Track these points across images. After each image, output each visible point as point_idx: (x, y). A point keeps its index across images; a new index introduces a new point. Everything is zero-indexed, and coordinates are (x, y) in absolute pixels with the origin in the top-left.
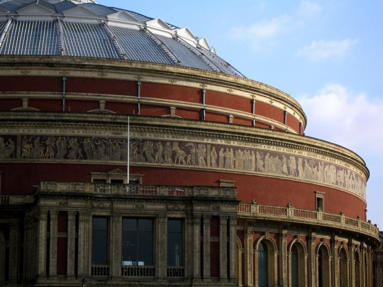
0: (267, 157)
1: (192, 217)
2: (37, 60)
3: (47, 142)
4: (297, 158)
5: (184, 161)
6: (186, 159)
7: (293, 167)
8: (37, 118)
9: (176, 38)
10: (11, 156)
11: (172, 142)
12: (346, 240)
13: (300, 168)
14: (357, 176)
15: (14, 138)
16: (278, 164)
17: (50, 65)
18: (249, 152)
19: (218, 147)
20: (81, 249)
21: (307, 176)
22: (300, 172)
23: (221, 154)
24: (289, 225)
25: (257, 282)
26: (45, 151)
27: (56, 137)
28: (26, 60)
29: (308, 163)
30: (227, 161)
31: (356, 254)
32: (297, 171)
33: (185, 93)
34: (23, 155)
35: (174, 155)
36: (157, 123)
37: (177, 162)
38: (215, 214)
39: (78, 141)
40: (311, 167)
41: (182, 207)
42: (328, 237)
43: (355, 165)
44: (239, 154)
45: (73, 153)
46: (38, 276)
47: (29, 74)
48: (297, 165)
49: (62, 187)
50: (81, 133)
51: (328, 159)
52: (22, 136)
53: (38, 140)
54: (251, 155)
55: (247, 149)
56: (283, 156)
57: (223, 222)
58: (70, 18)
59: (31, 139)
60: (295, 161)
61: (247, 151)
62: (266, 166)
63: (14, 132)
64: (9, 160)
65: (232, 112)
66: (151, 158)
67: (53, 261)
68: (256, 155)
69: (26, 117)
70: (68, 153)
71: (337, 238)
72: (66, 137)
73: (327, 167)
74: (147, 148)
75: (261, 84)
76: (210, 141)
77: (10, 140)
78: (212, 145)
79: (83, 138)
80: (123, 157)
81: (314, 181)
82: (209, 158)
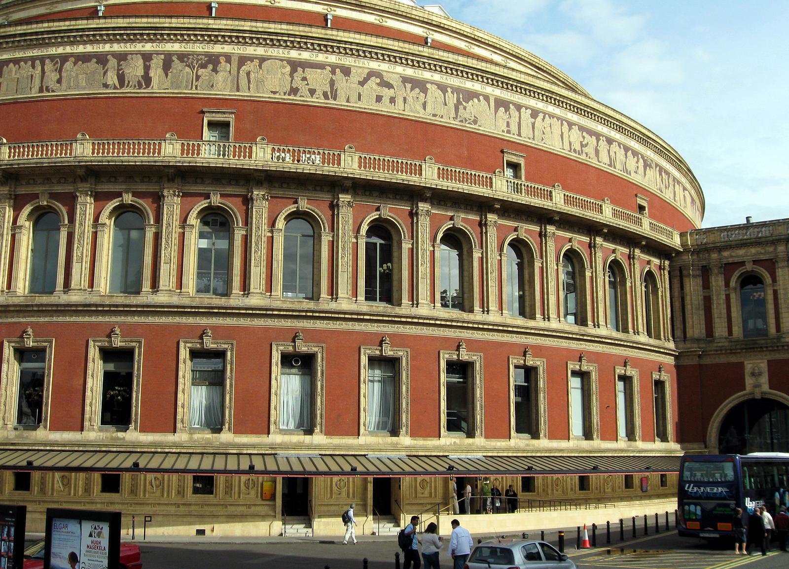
0: (68, 65)
4: (147, 57)
7: (135, 70)
13: (156, 73)
16: (93, 73)
18: (30, 63)
22: (155, 82)
29: (182, 61)
32: (147, 80)
40: (189, 66)
44: (11, 71)
48: (147, 68)
54: (33, 67)
55: (25, 60)
56: (109, 57)
60: (140, 62)
61: (26, 63)
62: (64, 80)
68: (43, 64)
73: (248, 67)
81: (202, 92)
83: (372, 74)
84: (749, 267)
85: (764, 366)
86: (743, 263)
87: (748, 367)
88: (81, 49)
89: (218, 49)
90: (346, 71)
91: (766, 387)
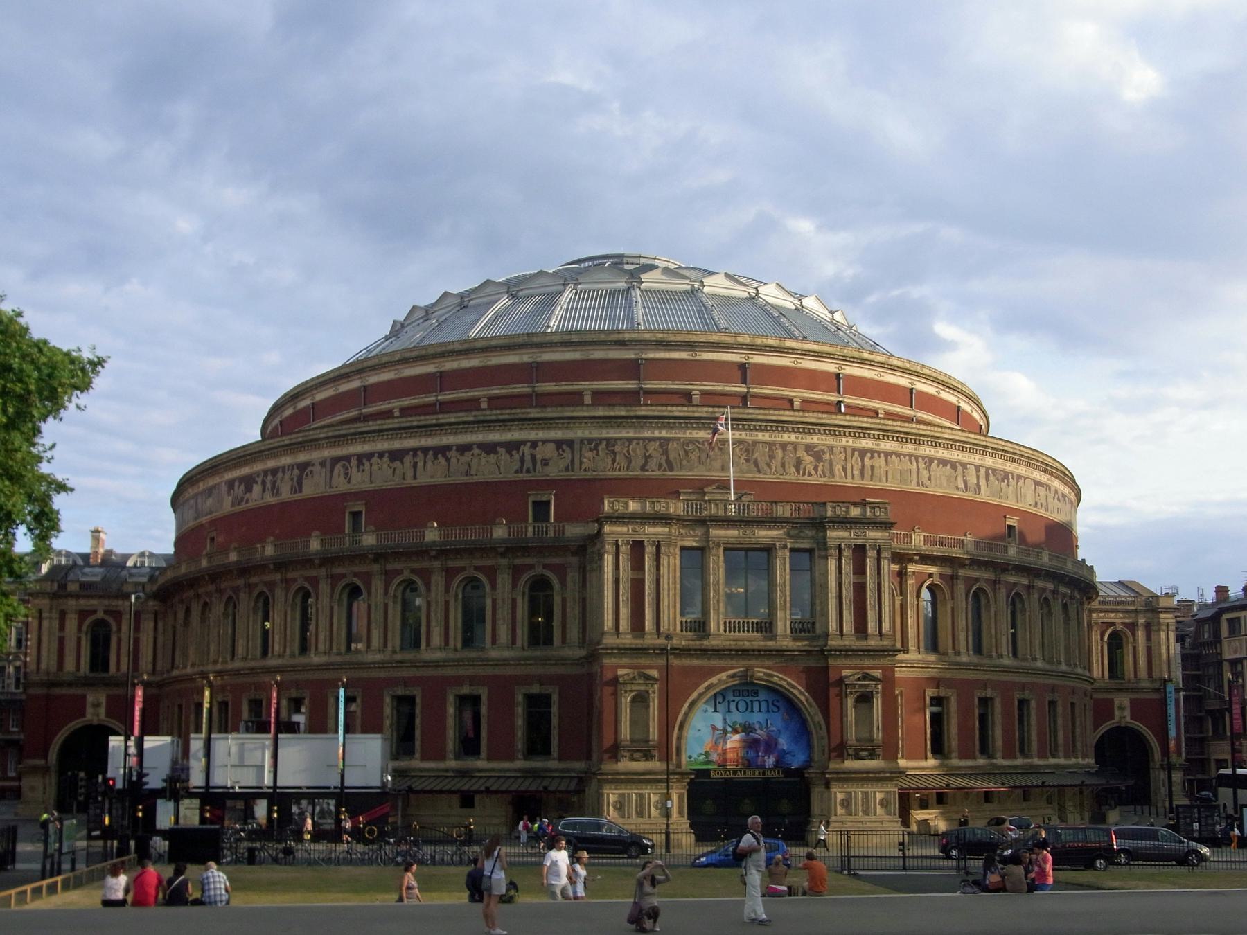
1: (823, 545)
2: (603, 337)
3: (617, 448)
4: (977, 468)
5: (813, 472)
6: (816, 469)
7: (972, 480)
8: (601, 414)
9: (800, 309)
10: (567, 469)
11: (795, 446)
12: (1051, 587)
13: (982, 482)
14: (1064, 496)
15: (570, 443)
17: (622, 343)
19: (863, 453)
20: (663, 595)
21: (993, 494)
22: (983, 488)
23: (866, 460)
24: (967, 562)
25: (922, 644)
26: (614, 461)
27: (630, 440)
28: (588, 338)
30: (876, 471)
31: (1065, 606)
33: (813, 379)
34: (583, 467)
35: (798, 463)
36: (774, 418)
37: (804, 474)
38: (860, 542)
39: (661, 446)
41: (809, 533)
42: (1024, 581)
43: (1061, 480)
44: (893, 462)
45: (653, 464)
46: (603, 634)
47: (592, 357)
48: (978, 477)
49: (633, 506)
50: (664, 434)
51: (1022, 470)
52: (582, 441)
53: (603, 445)
55: (905, 456)
57: (871, 554)
58: (651, 280)
59: (594, 444)
63: (570, 435)
64: (565, 475)
65: (882, 406)
66: (766, 468)
67: (624, 612)
69: (586, 414)
70: (646, 463)
71: (1040, 584)
72: (644, 439)
73: (1022, 481)
74: (760, 455)
75: (924, 366)
76: (850, 442)
77: (564, 447)
78: (854, 450)
79: (668, 440)
80: (725, 468)
82: (849, 467)
83: (1056, 491)
84: (1119, 627)
85: (1127, 703)
86: (1113, 624)
87: (1117, 703)
88: (942, 453)
89: (1009, 467)
90: (1049, 487)
91: (1128, 719)
